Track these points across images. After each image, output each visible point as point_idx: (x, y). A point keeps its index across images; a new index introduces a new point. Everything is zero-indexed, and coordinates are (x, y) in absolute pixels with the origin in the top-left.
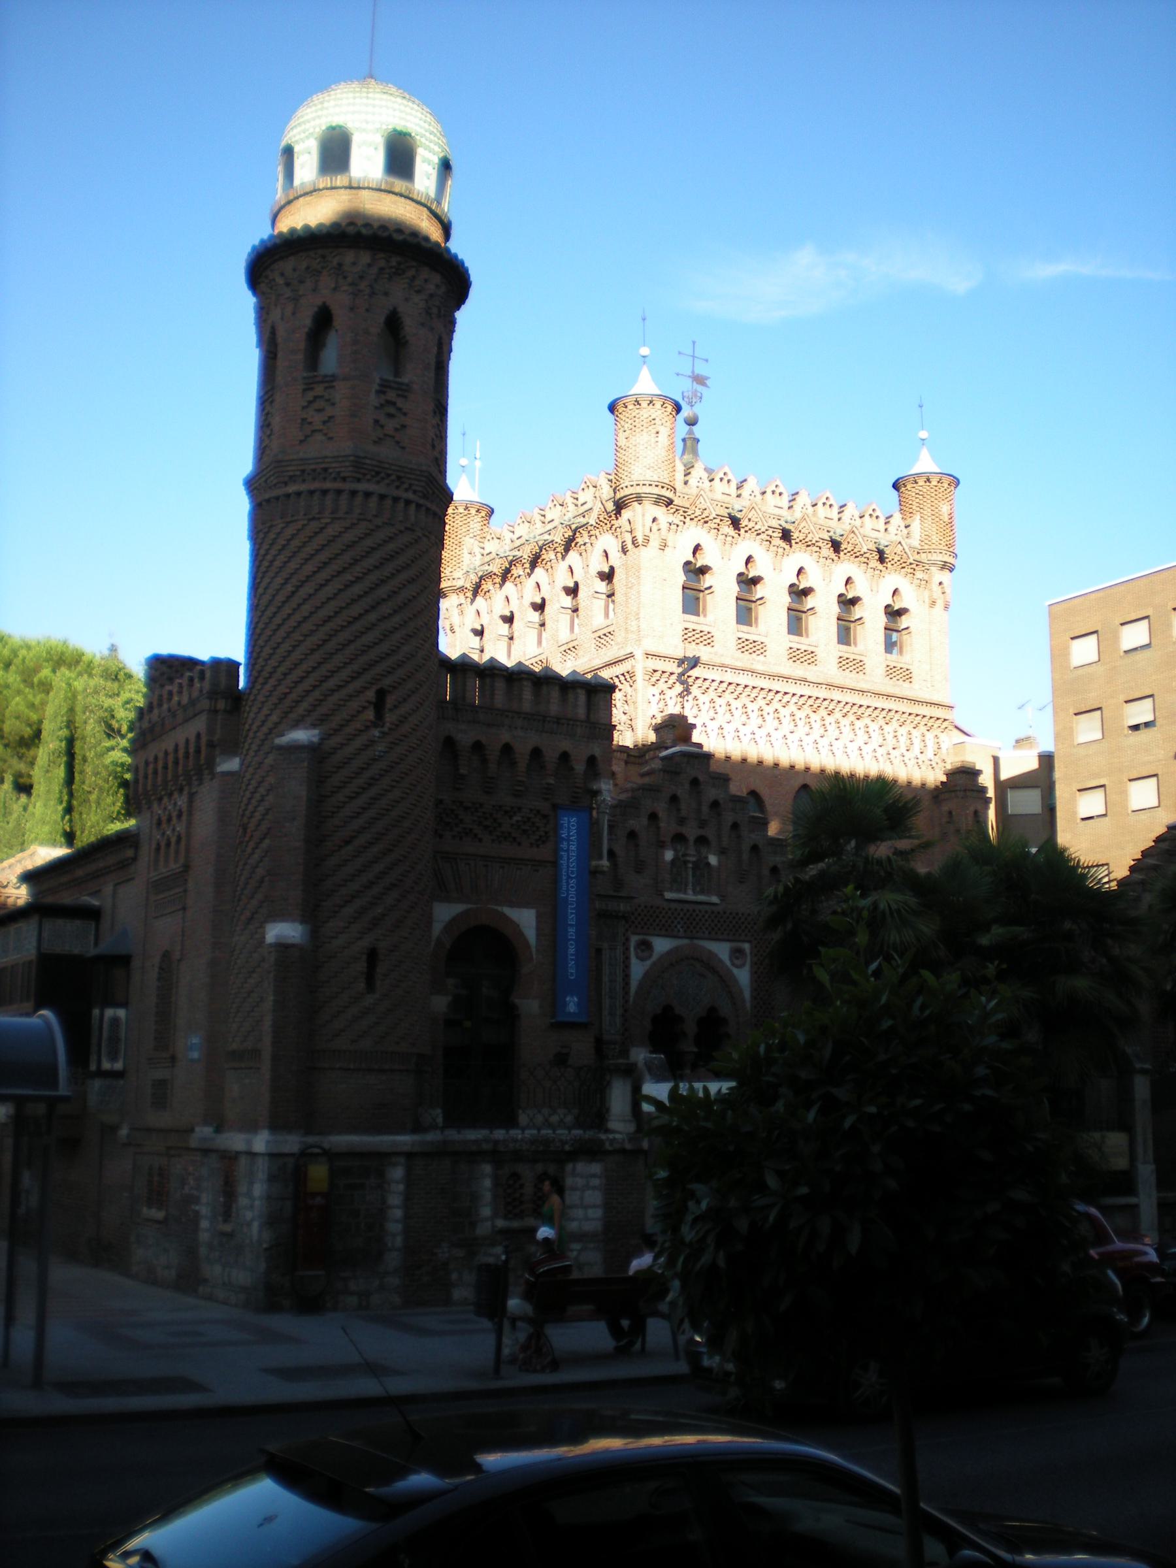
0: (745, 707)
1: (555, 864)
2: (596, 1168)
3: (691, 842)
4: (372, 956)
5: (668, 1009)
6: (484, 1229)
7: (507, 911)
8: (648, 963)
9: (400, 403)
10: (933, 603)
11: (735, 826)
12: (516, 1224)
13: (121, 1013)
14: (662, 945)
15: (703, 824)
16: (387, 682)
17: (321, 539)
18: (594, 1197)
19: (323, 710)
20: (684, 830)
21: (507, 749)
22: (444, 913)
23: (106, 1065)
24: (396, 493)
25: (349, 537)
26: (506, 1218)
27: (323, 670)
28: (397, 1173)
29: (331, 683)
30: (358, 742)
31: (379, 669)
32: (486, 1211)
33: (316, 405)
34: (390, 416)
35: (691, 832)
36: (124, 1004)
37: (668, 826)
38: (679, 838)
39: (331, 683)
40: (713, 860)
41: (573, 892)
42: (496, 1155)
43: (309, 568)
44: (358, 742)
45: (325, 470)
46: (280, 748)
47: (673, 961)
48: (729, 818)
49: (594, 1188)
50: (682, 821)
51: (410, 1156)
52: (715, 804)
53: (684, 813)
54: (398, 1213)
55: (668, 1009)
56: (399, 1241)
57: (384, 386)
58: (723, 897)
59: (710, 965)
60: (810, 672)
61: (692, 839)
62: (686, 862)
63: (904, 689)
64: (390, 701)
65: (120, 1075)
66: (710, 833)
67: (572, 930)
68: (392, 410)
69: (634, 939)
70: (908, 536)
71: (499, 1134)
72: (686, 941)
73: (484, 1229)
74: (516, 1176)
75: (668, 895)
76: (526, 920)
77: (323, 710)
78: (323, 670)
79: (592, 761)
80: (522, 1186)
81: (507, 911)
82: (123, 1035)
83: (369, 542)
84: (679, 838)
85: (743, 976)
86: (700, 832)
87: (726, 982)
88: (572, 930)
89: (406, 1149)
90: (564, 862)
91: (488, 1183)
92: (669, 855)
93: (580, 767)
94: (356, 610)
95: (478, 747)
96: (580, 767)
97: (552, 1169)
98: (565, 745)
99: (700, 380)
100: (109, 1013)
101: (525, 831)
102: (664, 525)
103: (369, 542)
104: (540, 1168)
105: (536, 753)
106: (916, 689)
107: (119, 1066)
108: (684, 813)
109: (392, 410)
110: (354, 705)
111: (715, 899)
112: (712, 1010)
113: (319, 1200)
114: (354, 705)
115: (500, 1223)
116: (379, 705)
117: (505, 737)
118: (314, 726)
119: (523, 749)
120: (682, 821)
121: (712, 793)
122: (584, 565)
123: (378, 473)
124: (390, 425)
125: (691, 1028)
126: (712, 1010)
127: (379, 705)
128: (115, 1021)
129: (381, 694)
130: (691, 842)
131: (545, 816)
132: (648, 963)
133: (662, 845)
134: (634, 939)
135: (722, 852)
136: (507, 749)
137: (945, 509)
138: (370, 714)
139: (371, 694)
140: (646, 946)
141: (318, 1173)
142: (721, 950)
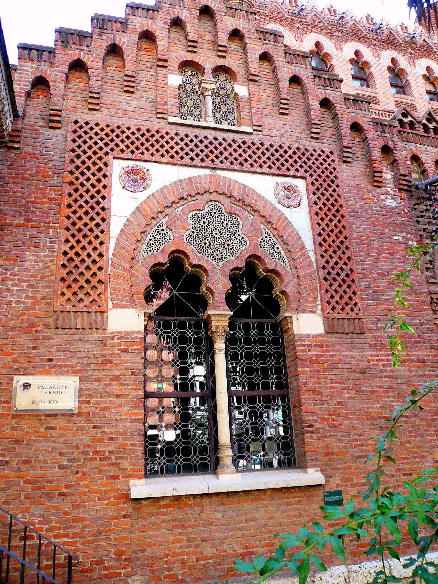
5: (177, 259)
8: (142, 197)
11: (265, 57)
14: (163, 175)
15: (221, 51)
20: (196, 58)
35: (208, 60)
40: (241, 90)
50: (192, 46)
52: (236, 34)
53: (191, 37)
55: (177, 259)
59: (246, 202)
61: (208, 68)
66: (233, 62)
69: (117, 167)
72: (208, 172)
92: (175, 80)
120: (192, 46)
125: (218, 283)
132: (142, 197)
133: (162, 63)
140: (136, 179)
142: (264, 186)
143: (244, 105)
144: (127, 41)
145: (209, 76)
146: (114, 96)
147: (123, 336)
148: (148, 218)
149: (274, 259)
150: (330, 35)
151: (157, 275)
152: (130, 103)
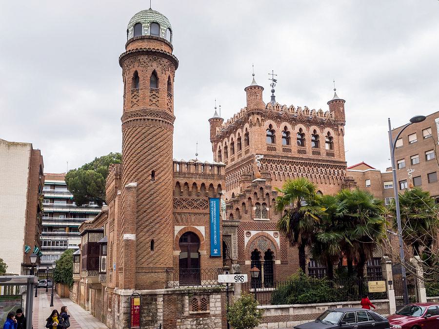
0: (285, 166)
1: (210, 214)
2: (219, 296)
3: (261, 205)
4: (152, 242)
5: (256, 250)
6: (186, 314)
7: (196, 227)
9: (157, 94)
10: (339, 135)
11: (274, 200)
12: (195, 312)
13: (105, 257)
14: (253, 233)
16: (154, 169)
17: (136, 132)
18: (219, 304)
19: (138, 177)
20: (259, 202)
21: (195, 184)
22: (178, 229)
23: (102, 271)
24: (156, 118)
25: (143, 131)
26: (193, 310)
27: (137, 167)
28: (160, 300)
29: (139, 170)
30: (147, 185)
31: (152, 165)
32: (187, 309)
33: (134, 97)
34: (154, 98)
35: (261, 202)
36: (106, 255)
37: (254, 201)
38: (258, 204)
39: (139, 170)
40: (268, 209)
41: (215, 221)
42: (189, 293)
43: (134, 140)
44: (147, 185)
45: (137, 114)
46: (126, 188)
47: (257, 237)
48: (271, 197)
49: (219, 302)
50: (258, 199)
51: (164, 295)
52: (267, 194)
53: (258, 197)
54: (162, 310)
55: (256, 250)
56: (162, 318)
57: (152, 90)
58: (271, 219)
59: (268, 237)
60: (304, 156)
61: (261, 204)
62: (260, 210)
63: (332, 158)
64: (156, 174)
65: (105, 273)
66: (266, 202)
67: (215, 231)
68: (155, 97)
69: (245, 232)
70: (331, 117)
71: (196, 287)
73: (186, 314)
74: (195, 299)
75: (255, 219)
76: (202, 230)
77: (138, 177)
78: (137, 167)
79: (219, 186)
80: (197, 302)
81: (196, 227)
82: (106, 263)
83: (149, 132)
84: (258, 204)
85: (278, 240)
86: (264, 202)
87: (273, 242)
88: (215, 231)
89: (163, 293)
90: (212, 213)
91: (187, 301)
92: (255, 208)
93: (216, 187)
94: (146, 150)
95: (186, 184)
96: (216, 187)
97: (205, 297)
98: (211, 182)
99: (275, 81)
100: (103, 257)
101: (201, 206)
102: (260, 120)
103: (149, 132)
104: (202, 297)
105: (203, 185)
106: (336, 158)
107: (105, 271)
108: (258, 197)
109: (155, 97)
110: (146, 175)
111: (268, 220)
112: (269, 250)
113: (137, 308)
114: (146, 175)
115: (191, 312)
116: (153, 175)
117: (194, 180)
118: (136, 181)
119: (199, 184)
120: (258, 199)
121: (266, 191)
122: (241, 132)
123: (151, 114)
124: (154, 100)
125: (263, 255)
126: (269, 250)
127: (153, 175)
128: (104, 259)
129: (153, 173)
130: (261, 205)
131: (207, 201)
133: (252, 206)
134: (245, 232)
135: (270, 207)
136: (195, 184)
137: (341, 109)
138: (150, 177)
139: (150, 172)
140: (249, 233)
141: (137, 301)
143: (268, 213)
144: (246, 201)
145: (261, 207)
146: (244, 215)
147: (248, 265)
148: (251, 242)
149: (272, 250)
150: (290, 123)
151: (252, 253)
152: (247, 216)
